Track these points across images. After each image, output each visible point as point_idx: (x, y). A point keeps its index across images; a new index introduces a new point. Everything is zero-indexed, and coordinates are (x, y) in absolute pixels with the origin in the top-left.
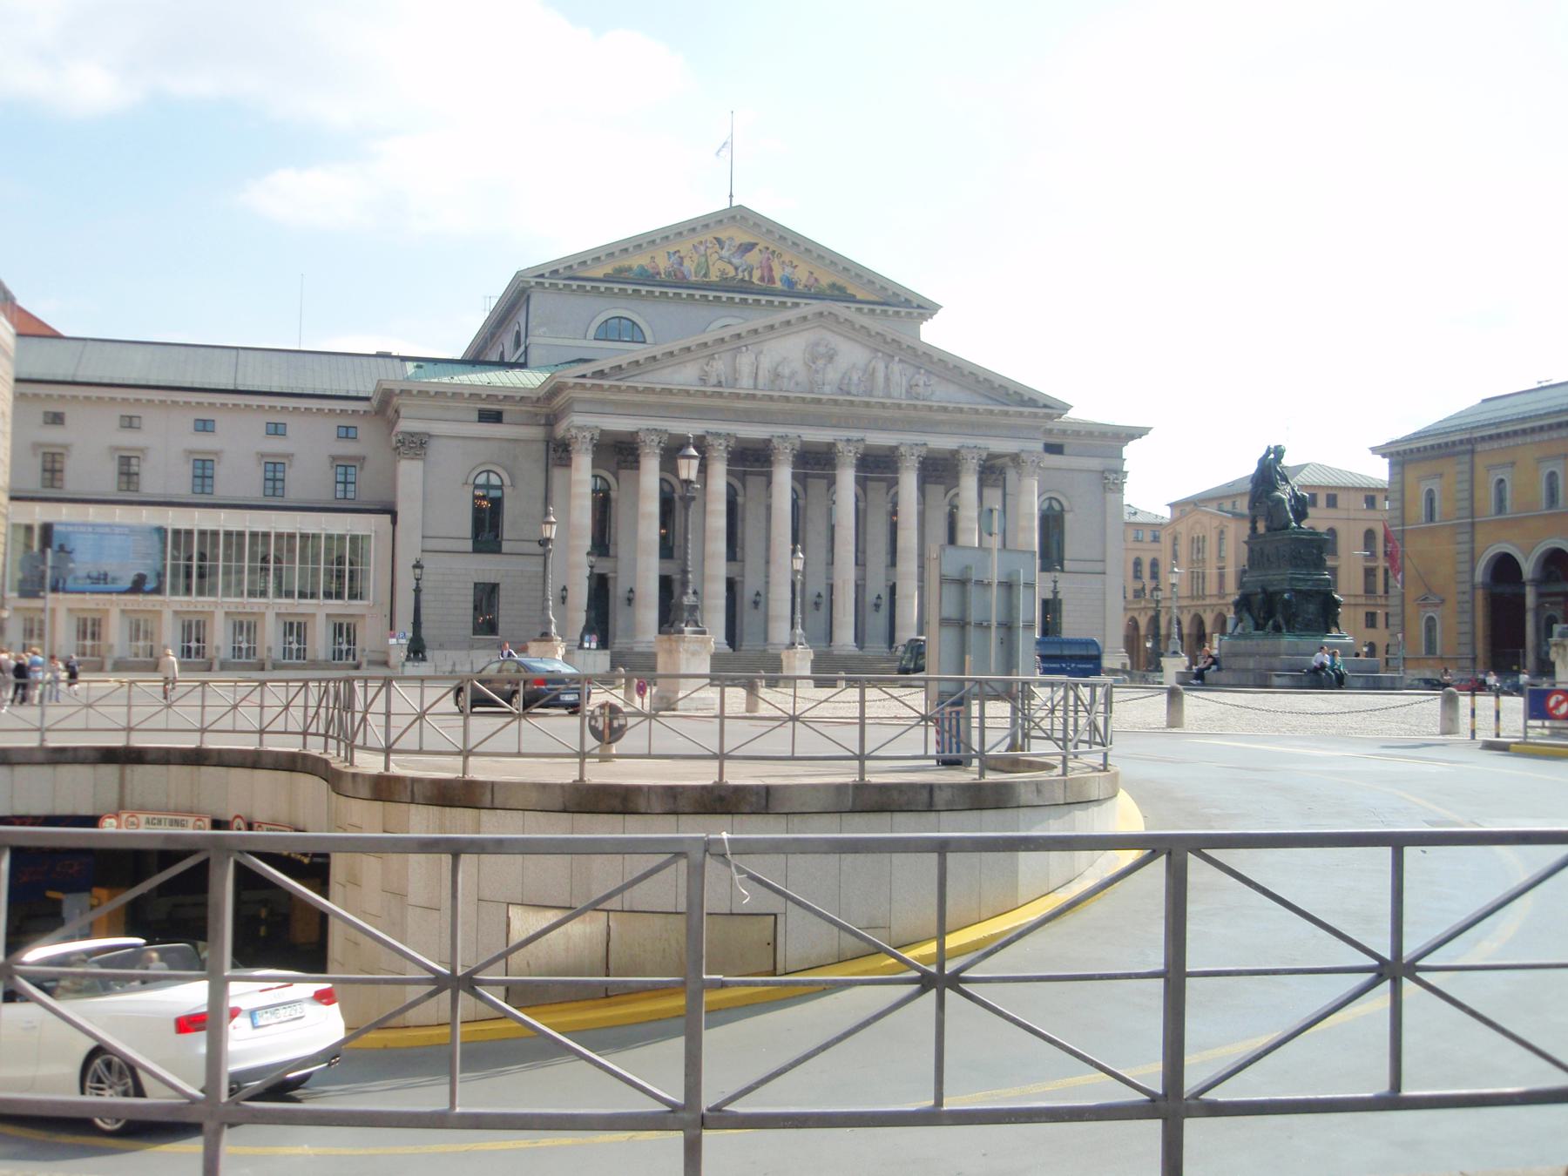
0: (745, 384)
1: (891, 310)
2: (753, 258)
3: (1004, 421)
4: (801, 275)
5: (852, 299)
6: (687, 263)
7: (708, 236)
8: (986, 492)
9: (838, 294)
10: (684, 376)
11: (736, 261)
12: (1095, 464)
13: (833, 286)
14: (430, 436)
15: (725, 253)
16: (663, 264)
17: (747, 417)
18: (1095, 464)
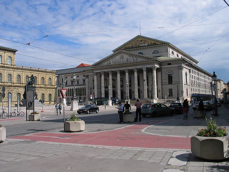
0: (112, 63)
1: (162, 45)
2: (142, 42)
3: (148, 62)
4: (149, 43)
5: (157, 45)
6: (134, 45)
7: (136, 40)
8: (158, 73)
9: (155, 44)
10: (105, 64)
11: (140, 43)
12: (177, 65)
13: (154, 43)
14: (88, 75)
15: (139, 42)
16: (131, 46)
17: (113, 68)
18: (177, 65)
